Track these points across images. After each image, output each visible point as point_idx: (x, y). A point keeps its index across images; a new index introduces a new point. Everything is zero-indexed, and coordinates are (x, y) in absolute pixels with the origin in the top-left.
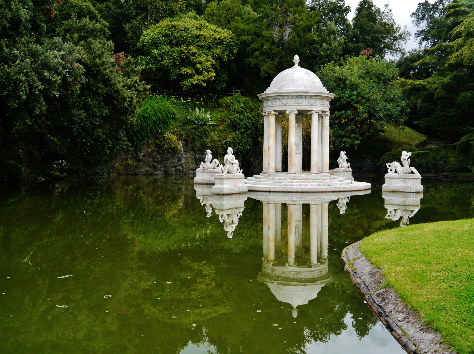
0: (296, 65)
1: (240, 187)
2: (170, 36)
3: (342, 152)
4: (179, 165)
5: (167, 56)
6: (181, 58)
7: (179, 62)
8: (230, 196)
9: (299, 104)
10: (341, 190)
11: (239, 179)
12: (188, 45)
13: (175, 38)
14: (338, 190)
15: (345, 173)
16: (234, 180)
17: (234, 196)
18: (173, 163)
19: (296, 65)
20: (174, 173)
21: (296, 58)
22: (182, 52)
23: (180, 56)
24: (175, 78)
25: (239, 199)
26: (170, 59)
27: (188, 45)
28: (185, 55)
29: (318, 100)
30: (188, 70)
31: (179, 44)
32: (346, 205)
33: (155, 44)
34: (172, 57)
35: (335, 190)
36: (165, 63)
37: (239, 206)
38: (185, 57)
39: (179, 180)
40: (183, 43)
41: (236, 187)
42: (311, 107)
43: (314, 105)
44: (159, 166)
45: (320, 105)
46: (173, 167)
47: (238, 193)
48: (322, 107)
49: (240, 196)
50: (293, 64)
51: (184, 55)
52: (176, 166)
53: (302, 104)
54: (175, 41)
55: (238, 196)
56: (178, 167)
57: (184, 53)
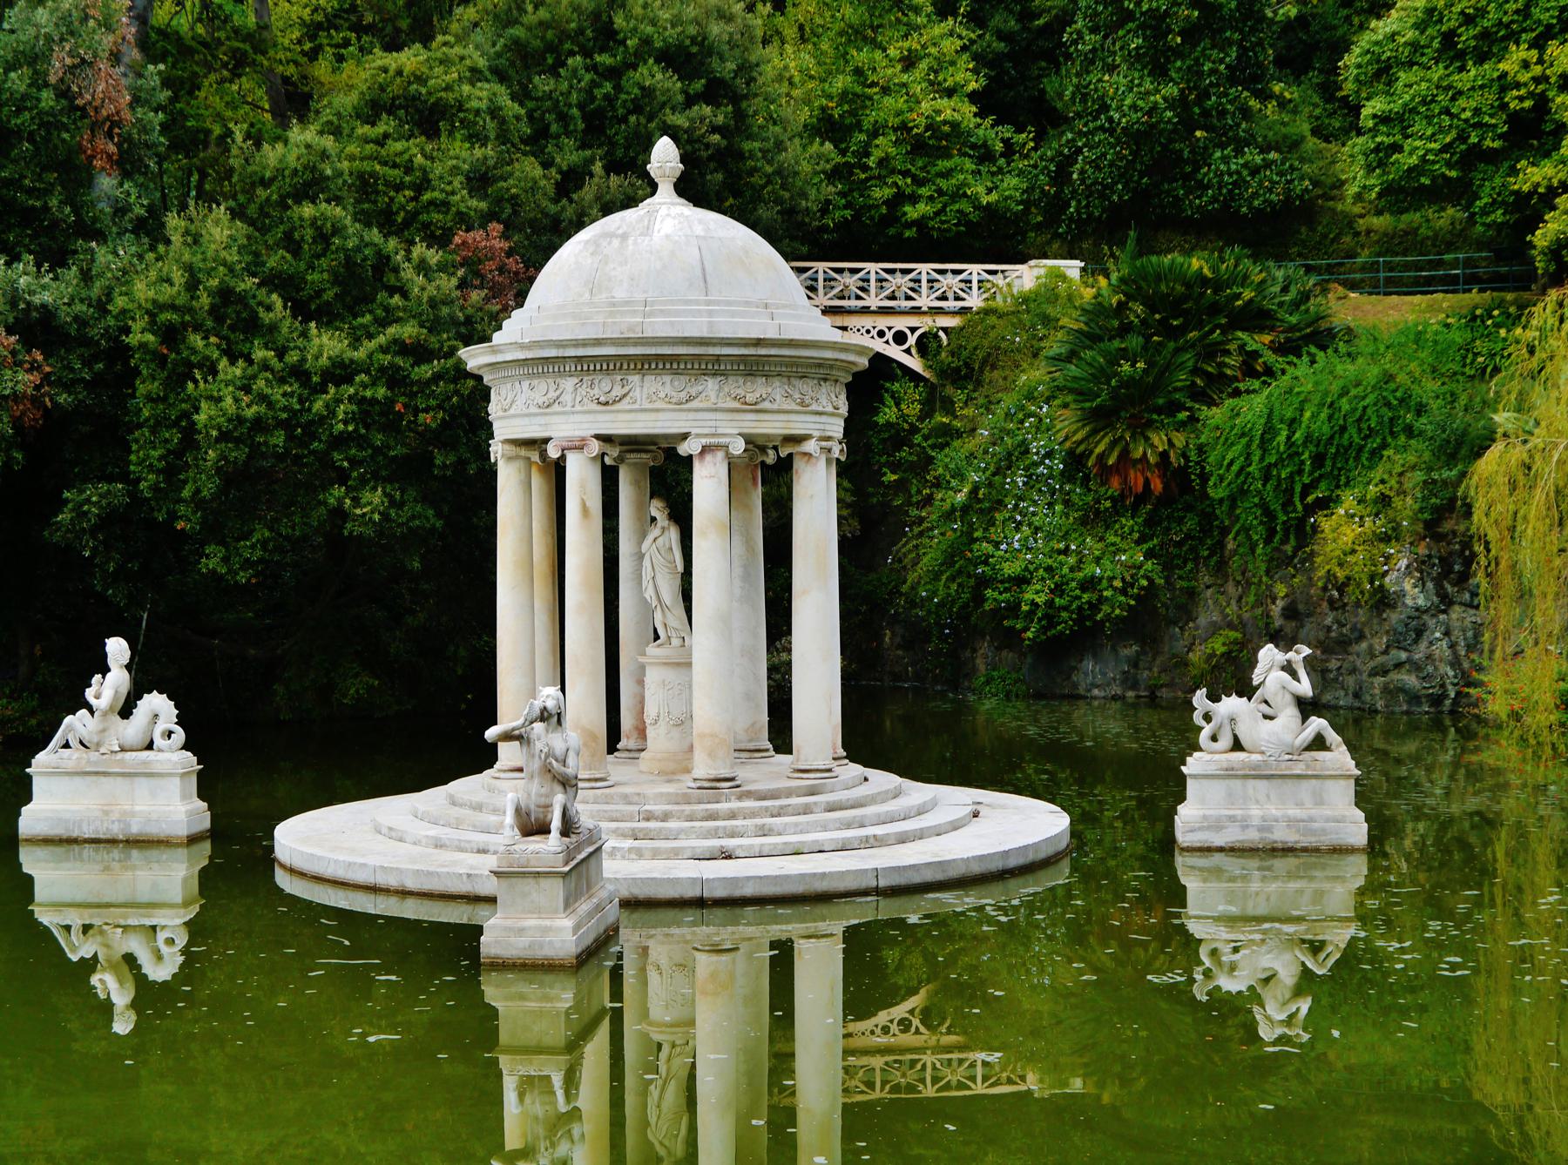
0: (666, 192)
1: (133, 814)
2: (1440, 21)
3: (1269, 654)
5: (1429, 119)
6: (1515, 118)
7: (1501, 136)
8: (59, 850)
10: (411, 884)
11: (143, 780)
12: (1539, 44)
13: (1468, 20)
14: (392, 881)
15: (1262, 785)
16: (103, 779)
17: (88, 850)
18: (1371, 654)
19: (666, 192)
20: (1380, 705)
21: (664, 156)
22: (1504, 83)
23: (1504, 106)
24: (1498, 216)
25: (127, 869)
26: (1441, 130)
27: (1539, 44)
28: (1531, 95)
29: (569, 384)
30: (1535, 175)
31: (1490, 46)
32: (1298, 992)
33: (1382, 72)
34: (1452, 116)
35: (382, 880)
36: (1411, 154)
37: (145, 899)
38: (1528, 104)
39: (1403, 736)
40: (1514, 37)
41: (106, 813)
42: (542, 420)
45: (595, 407)
46: (1374, 673)
47: (113, 842)
48: (600, 417)
49: (129, 857)
51: (1521, 99)
52: (1385, 673)
53: (512, 411)
54: (1466, 37)
55: (116, 853)
56: (1394, 676)
57: (1518, 85)
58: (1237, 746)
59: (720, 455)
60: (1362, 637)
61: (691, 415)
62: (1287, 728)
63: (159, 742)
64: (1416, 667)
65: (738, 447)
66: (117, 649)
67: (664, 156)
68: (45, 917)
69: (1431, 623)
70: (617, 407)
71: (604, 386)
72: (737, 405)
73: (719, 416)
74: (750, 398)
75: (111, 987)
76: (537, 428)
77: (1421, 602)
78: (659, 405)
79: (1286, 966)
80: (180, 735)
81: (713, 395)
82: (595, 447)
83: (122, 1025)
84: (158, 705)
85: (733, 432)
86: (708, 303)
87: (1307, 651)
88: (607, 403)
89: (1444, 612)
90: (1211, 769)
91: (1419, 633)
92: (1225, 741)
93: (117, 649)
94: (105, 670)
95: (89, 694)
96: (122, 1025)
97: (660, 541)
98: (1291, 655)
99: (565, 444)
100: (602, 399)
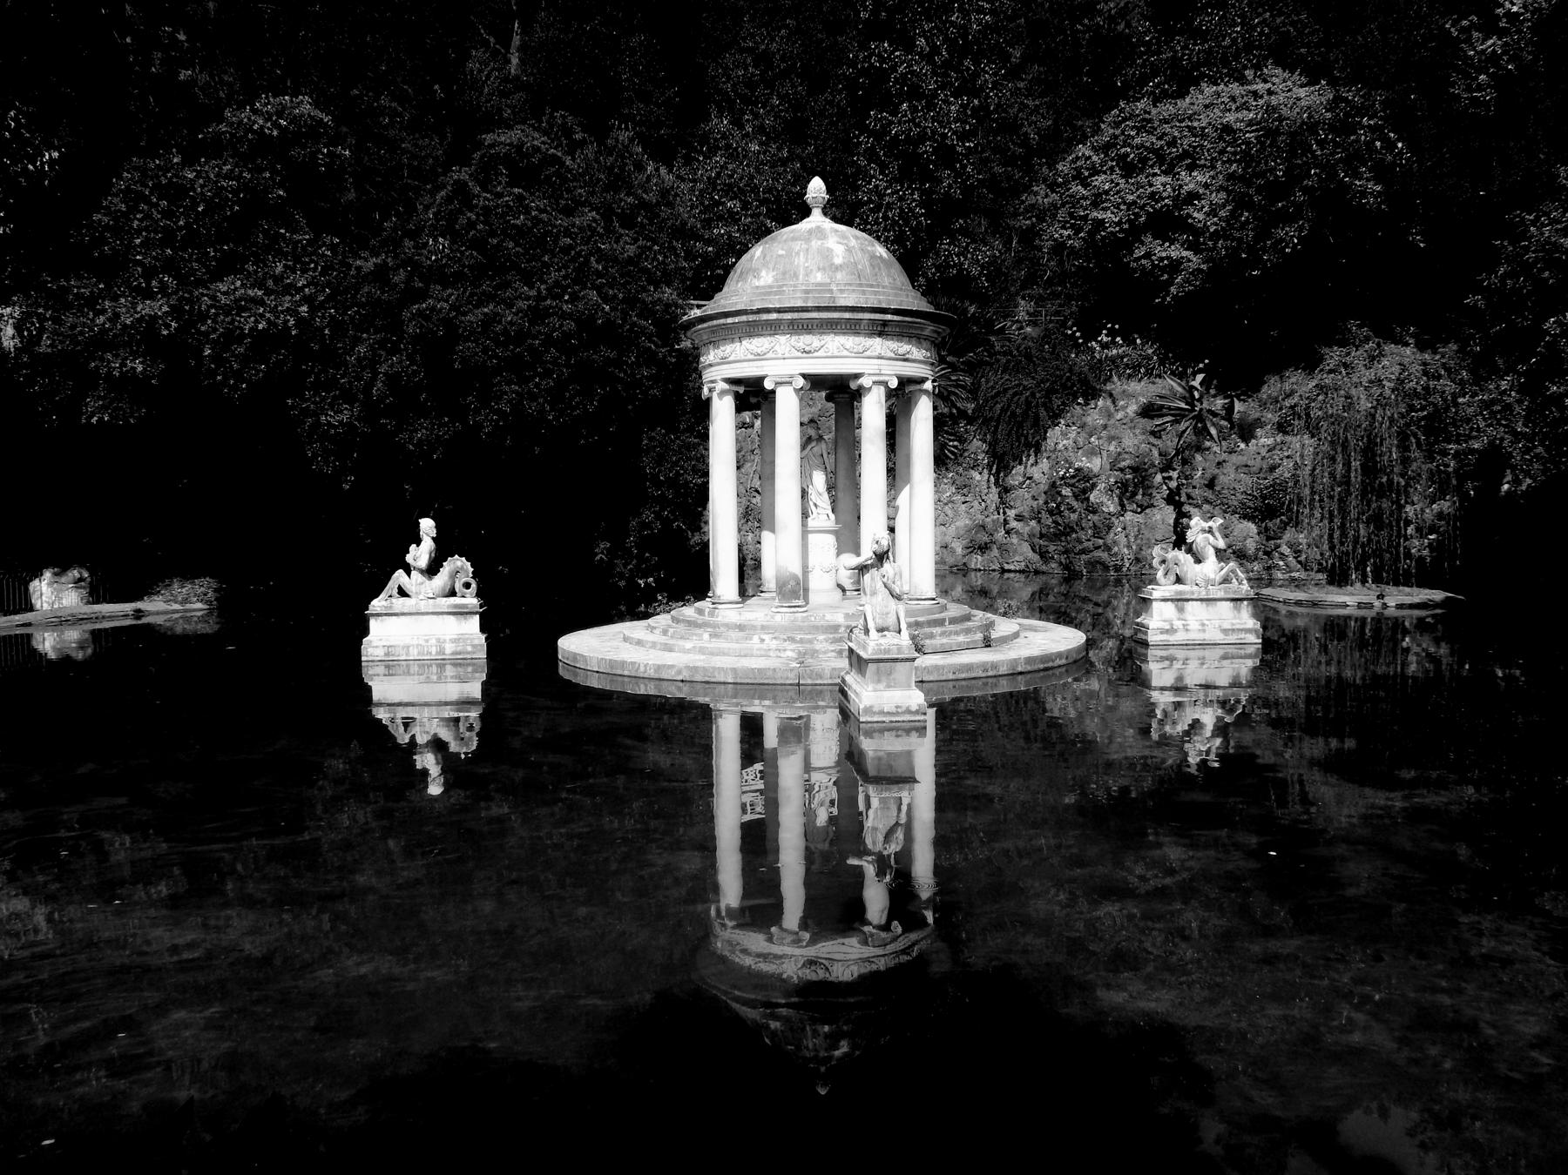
4: (1098, 548)
9: (724, 361)
21: (816, 188)
29: (783, 339)
43: (770, 355)
44: (1052, 548)
45: (800, 354)
50: (805, 212)
58: (1179, 580)
59: (882, 389)
60: (1073, 530)
61: (866, 361)
62: (1211, 567)
63: (458, 586)
64: (1108, 549)
65: (894, 384)
66: (427, 525)
67: (816, 188)
68: (381, 714)
69: (1116, 522)
70: (816, 354)
71: (806, 340)
72: (893, 355)
73: (883, 361)
74: (901, 351)
75: (427, 761)
76: (755, 369)
77: (1112, 509)
78: (845, 353)
79: (1208, 718)
80: (474, 585)
81: (879, 347)
82: (801, 382)
83: (435, 789)
84: (458, 565)
85: (892, 372)
86: (861, 285)
87: (1221, 521)
88: (809, 352)
89: (1123, 515)
90: (1167, 595)
91: (1110, 528)
92: (1173, 578)
93: (427, 525)
94: (418, 542)
95: (409, 558)
96: (435, 789)
97: (815, 449)
98: (1211, 523)
99: (779, 380)
100: (807, 349)
